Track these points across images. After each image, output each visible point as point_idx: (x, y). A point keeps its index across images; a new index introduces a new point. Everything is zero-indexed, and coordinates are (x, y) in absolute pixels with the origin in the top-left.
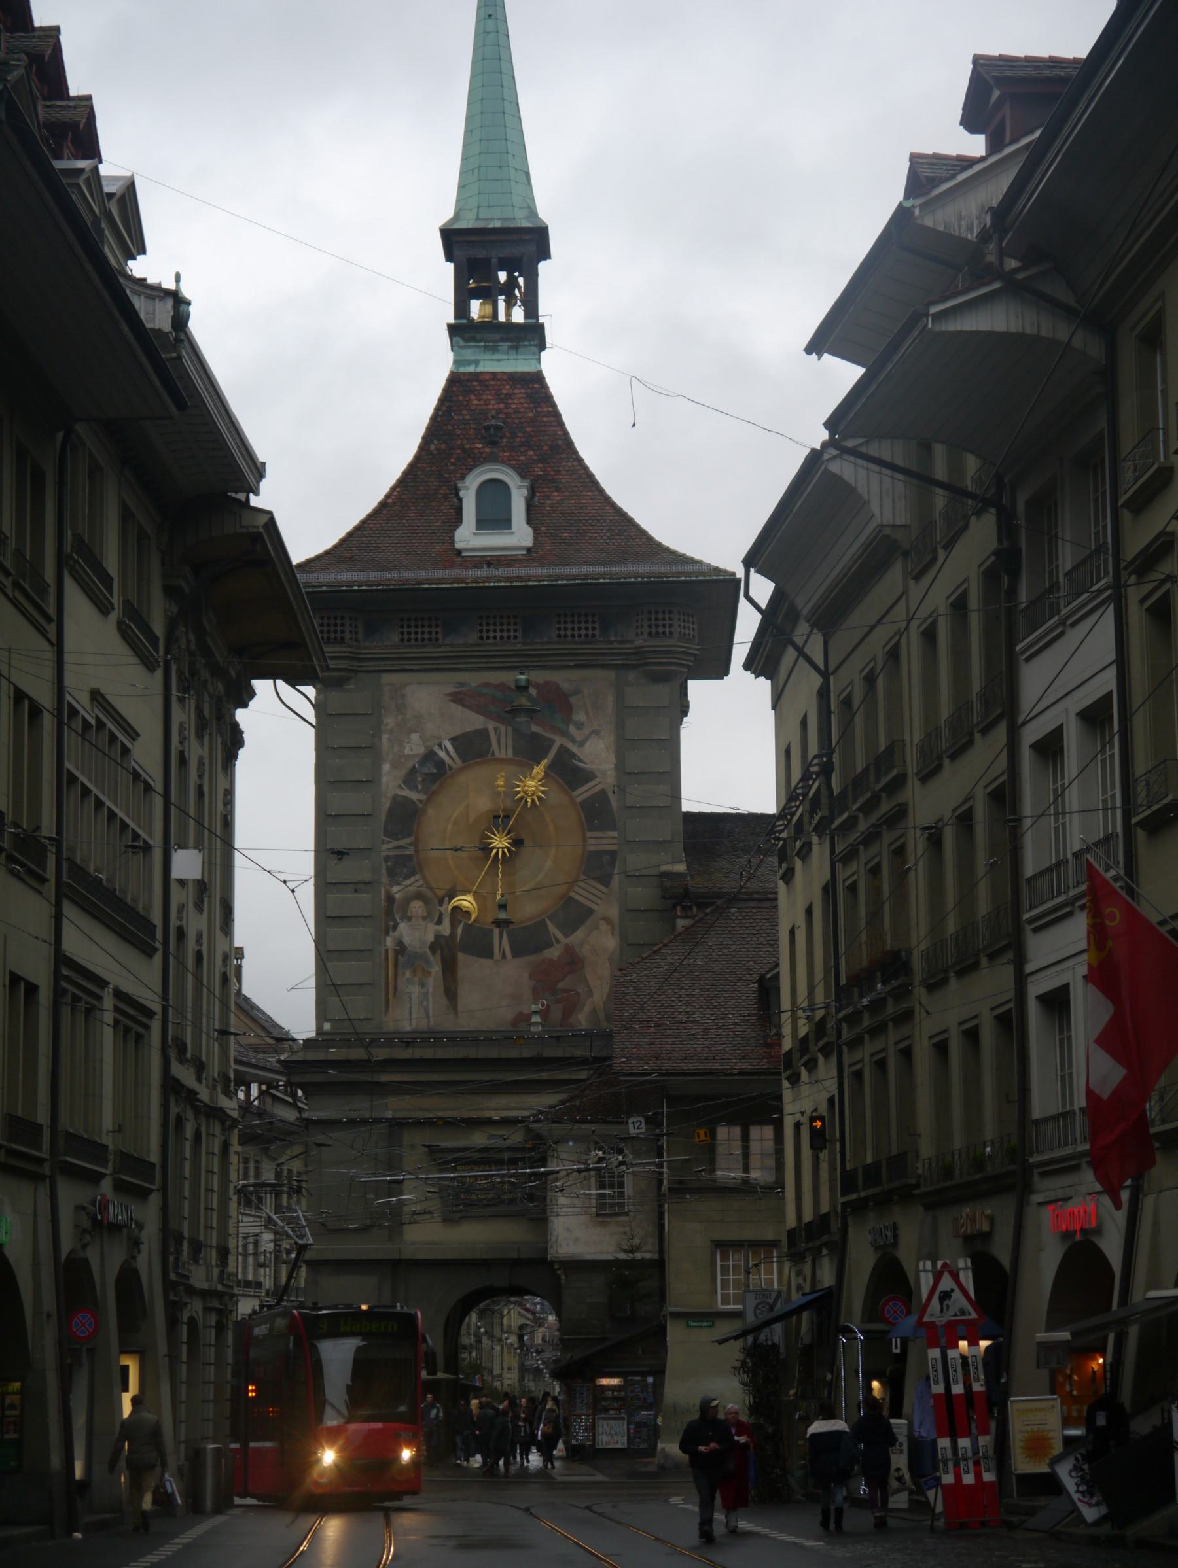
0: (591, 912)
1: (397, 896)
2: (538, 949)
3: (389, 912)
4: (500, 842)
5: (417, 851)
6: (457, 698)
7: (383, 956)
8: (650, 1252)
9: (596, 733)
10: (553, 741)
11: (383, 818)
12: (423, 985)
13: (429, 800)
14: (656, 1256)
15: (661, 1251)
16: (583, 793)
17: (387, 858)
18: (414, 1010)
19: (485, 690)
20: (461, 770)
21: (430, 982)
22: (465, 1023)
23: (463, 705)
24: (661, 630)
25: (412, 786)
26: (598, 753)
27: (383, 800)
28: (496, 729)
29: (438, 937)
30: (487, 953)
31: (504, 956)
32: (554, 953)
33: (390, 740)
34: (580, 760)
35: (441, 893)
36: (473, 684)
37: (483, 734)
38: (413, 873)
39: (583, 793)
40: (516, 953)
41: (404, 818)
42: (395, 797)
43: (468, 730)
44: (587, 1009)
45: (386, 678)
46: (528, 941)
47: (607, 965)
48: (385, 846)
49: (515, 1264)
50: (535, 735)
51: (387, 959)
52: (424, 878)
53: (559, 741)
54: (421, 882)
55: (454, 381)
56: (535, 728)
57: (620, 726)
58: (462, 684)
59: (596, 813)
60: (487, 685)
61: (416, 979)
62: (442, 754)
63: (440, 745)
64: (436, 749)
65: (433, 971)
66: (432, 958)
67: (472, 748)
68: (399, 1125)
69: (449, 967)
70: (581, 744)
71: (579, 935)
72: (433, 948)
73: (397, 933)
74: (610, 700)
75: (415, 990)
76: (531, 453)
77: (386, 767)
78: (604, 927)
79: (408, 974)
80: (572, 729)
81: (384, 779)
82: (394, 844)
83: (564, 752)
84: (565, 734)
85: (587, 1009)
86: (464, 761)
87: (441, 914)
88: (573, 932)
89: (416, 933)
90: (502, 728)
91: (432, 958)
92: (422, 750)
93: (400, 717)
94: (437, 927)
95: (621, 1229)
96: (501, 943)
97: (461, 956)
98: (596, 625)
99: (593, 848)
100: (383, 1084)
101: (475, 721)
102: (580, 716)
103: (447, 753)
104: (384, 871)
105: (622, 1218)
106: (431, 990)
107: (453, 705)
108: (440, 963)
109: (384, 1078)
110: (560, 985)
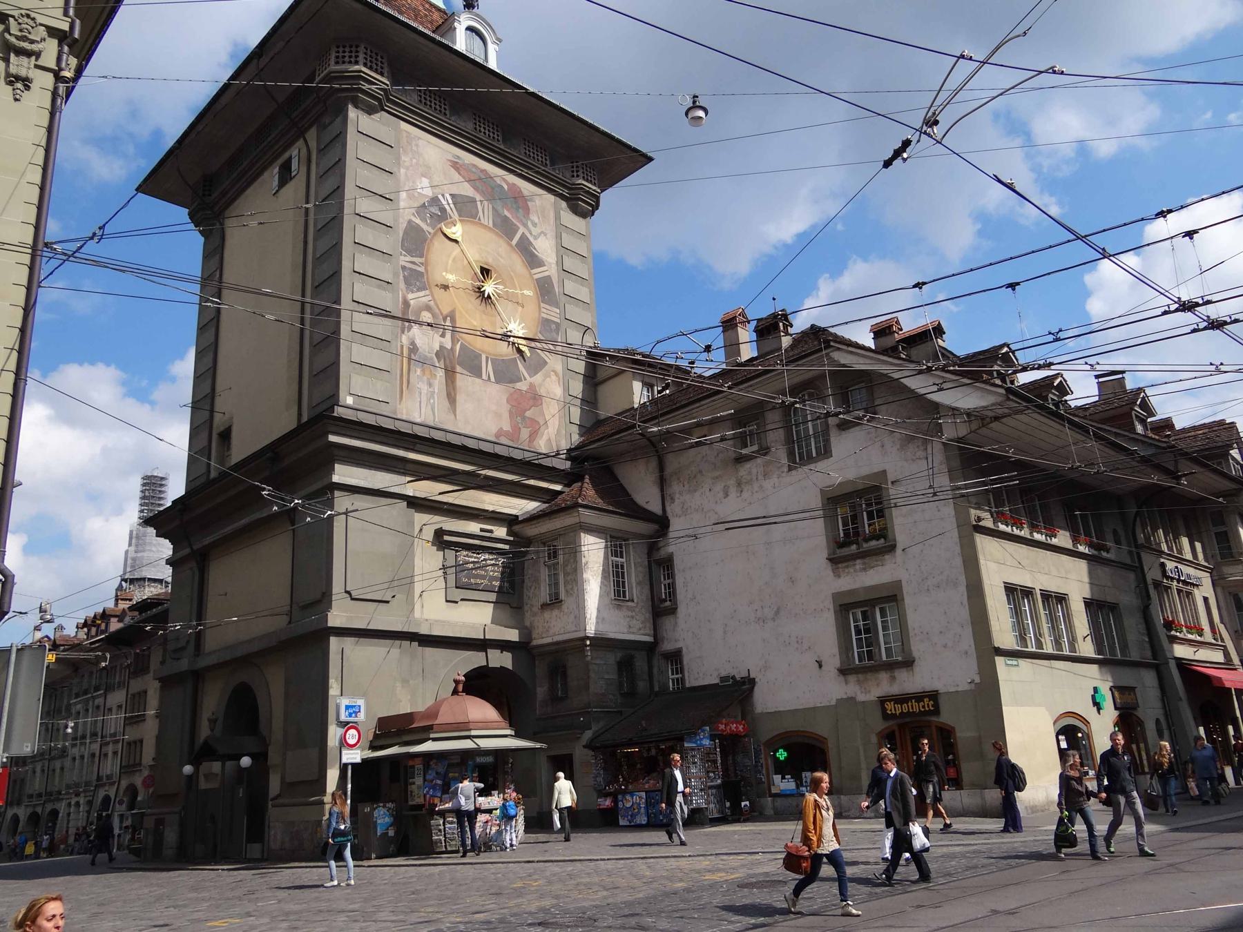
0: (546, 363)
1: (412, 302)
2: (512, 381)
6: (456, 166)
12: (430, 385)
15: (655, 636)
16: (538, 273)
17: (404, 268)
18: (423, 405)
25: (424, 220)
26: (545, 247)
30: (476, 371)
32: (522, 386)
35: (445, 312)
37: (473, 201)
38: (425, 289)
41: (415, 242)
44: (545, 437)
45: (403, 125)
48: (402, 258)
53: (522, 230)
54: (430, 298)
56: (506, 213)
57: (559, 237)
59: (545, 289)
62: (444, 202)
64: (440, 197)
68: (416, 504)
69: (450, 374)
70: (536, 238)
71: (538, 378)
72: (437, 354)
73: (411, 333)
74: (552, 214)
75: (424, 388)
77: (403, 195)
78: (554, 377)
79: (419, 371)
81: (402, 204)
82: (409, 258)
83: (523, 237)
84: (525, 226)
85: (545, 437)
88: (536, 373)
92: (430, 194)
96: (488, 369)
101: (467, 190)
102: (534, 218)
103: (447, 202)
105: (630, 604)
110: (528, 414)
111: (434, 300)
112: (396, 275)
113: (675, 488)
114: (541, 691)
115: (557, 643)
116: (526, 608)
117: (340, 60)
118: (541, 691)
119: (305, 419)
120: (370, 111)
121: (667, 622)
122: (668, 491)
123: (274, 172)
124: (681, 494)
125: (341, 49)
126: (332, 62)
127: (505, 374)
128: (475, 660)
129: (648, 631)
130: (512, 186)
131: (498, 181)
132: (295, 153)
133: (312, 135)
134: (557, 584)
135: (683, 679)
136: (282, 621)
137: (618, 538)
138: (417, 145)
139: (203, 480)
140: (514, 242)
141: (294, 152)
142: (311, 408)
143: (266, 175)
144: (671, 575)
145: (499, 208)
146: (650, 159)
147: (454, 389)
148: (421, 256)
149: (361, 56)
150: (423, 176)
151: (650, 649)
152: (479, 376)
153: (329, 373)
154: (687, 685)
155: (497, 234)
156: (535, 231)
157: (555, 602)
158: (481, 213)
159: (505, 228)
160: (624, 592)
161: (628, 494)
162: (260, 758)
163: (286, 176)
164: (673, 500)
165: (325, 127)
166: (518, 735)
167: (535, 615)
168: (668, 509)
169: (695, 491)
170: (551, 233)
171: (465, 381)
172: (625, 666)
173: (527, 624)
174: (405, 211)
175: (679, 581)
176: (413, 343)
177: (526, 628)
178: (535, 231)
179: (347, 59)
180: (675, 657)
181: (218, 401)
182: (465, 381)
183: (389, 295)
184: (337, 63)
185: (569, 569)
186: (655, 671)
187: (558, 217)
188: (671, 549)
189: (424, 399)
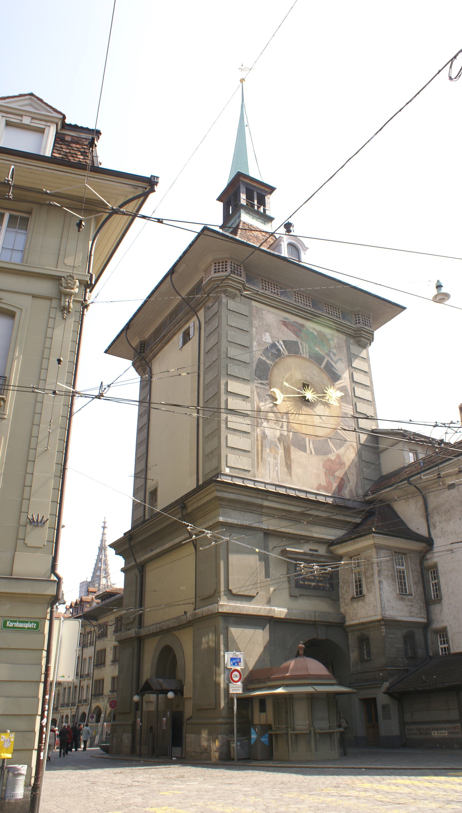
6: (285, 323)
7: (255, 439)
8: (424, 618)
9: (341, 360)
11: (254, 368)
12: (275, 458)
13: (274, 365)
14: (424, 620)
18: (271, 472)
19: (296, 325)
20: (287, 356)
21: (279, 457)
23: (287, 328)
24: (367, 323)
25: (268, 357)
27: (254, 359)
28: (301, 344)
29: (281, 435)
30: (303, 448)
31: (311, 453)
32: (332, 457)
33: (256, 332)
37: (296, 343)
40: (316, 454)
43: (290, 340)
45: (254, 303)
47: (355, 468)
49: (329, 625)
51: (257, 440)
58: (286, 318)
61: (272, 454)
62: (280, 347)
63: (278, 342)
65: (280, 453)
66: (279, 445)
70: (336, 363)
71: (342, 451)
72: (280, 439)
75: (271, 460)
77: (255, 344)
78: (352, 450)
79: (268, 450)
81: (254, 349)
83: (328, 363)
84: (328, 355)
85: (348, 489)
89: (272, 431)
91: (279, 445)
92: (271, 342)
93: (261, 323)
95: (410, 603)
96: (310, 446)
97: (292, 448)
99: (345, 411)
100: (261, 506)
101: (292, 337)
103: (282, 347)
104: (255, 393)
105: (410, 597)
106: (279, 462)
107: (283, 327)
108: (283, 449)
109: (266, 503)
112: (252, 392)
113: (435, 518)
114: (354, 655)
115: (363, 624)
116: (341, 600)
117: (217, 271)
118: (354, 655)
119: (201, 482)
120: (233, 297)
121: (435, 609)
122: (431, 521)
123: (179, 337)
124: (440, 522)
125: (217, 265)
126: (212, 272)
127: (322, 449)
128: (311, 635)
129: (423, 615)
130: (320, 332)
132: (192, 324)
133: (201, 313)
134: (361, 586)
135: (448, 648)
136: (190, 609)
137: (399, 553)
138: (262, 314)
139: (142, 520)
140: (322, 366)
141: (191, 324)
142: (204, 475)
143: (175, 338)
144: (436, 577)
146: (404, 308)
147: (290, 460)
148: (267, 379)
149: (229, 267)
150: (266, 331)
151: (426, 626)
152: (305, 451)
153: (215, 454)
154: (452, 652)
155: (312, 362)
156: (335, 359)
157: (360, 595)
158: (301, 351)
160: (406, 589)
161: (406, 525)
162: (179, 692)
163: (186, 338)
164: (435, 527)
165: (209, 308)
166: (340, 684)
167: (347, 605)
168: (432, 533)
169: (449, 520)
170: (345, 359)
172: (409, 638)
173: (342, 610)
174: (257, 353)
175: (443, 581)
176: (264, 433)
177: (342, 614)
178: (335, 359)
179: (221, 270)
180: (443, 633)
181: (149, 472)
182: (295, 454)
183: (249, 404)
184: (215, 272)
185: (368, 574)
186: (430, 642)
187: (348, 349)
188: (435, 560)
189: (272, 467)
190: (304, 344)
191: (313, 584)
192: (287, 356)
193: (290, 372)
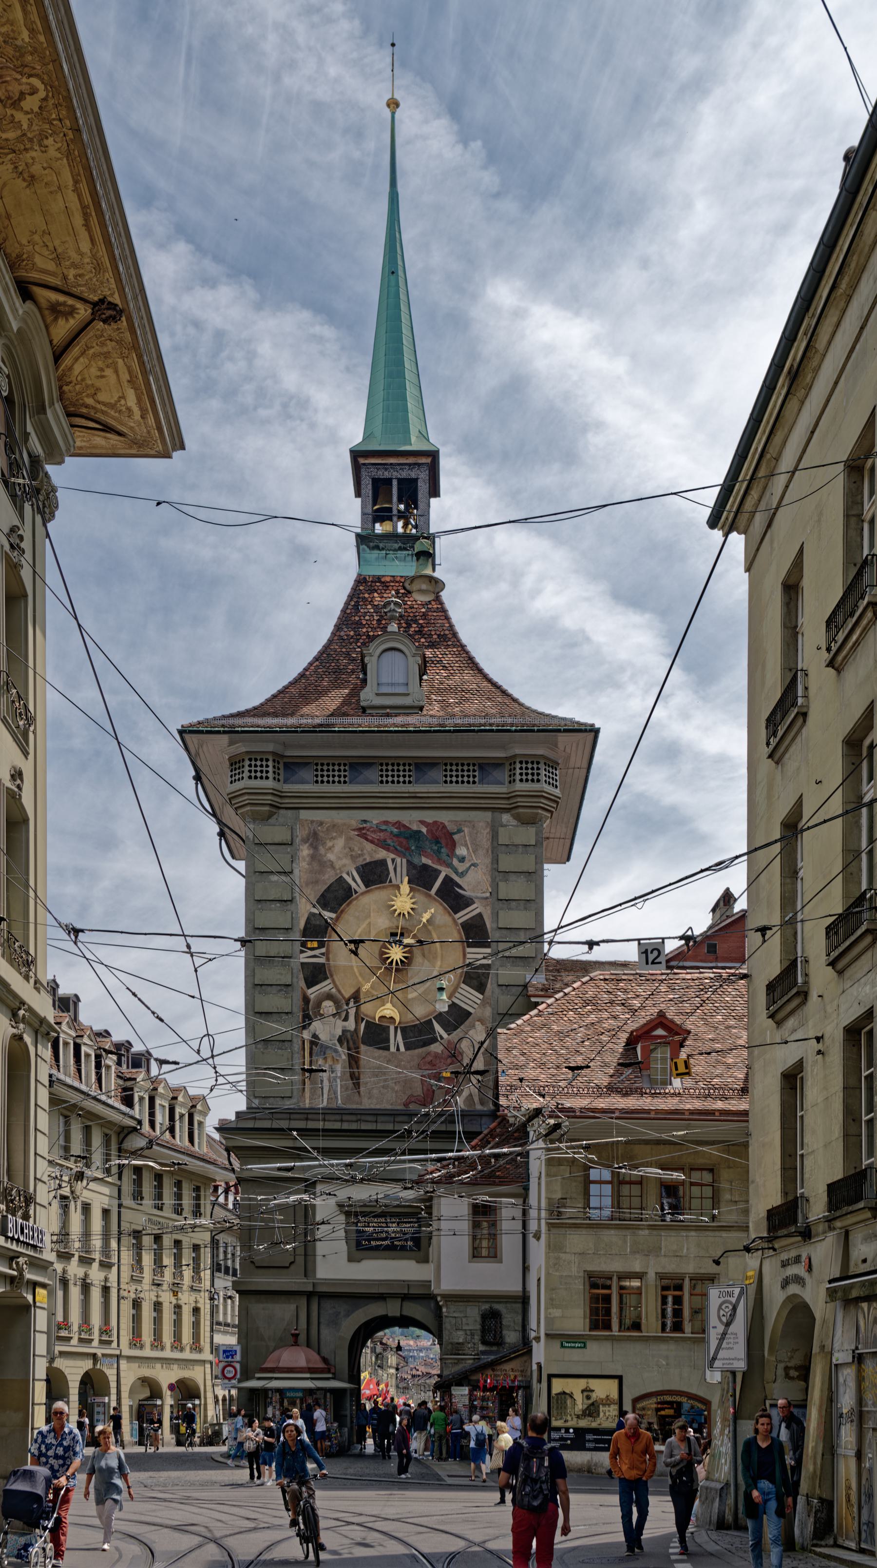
1: (312, 997)
3: (305, 1010)
4: (396, 953)
5: (328, 959)
10: (440, 872)
16: (464, 915)
19: (384, 827)
20: (363, 894)
22: (367, 1104)
28: (393, 860)
31: (398, 1049)
34: (460, 887)
35: (347, 996)
36: (375, 822)
37: (383, 863)
39: (464, 915)
42: (312, 915)
46: (418, 1034)
50: (425, 865)
52: (334, 982)
54: (331, 986)
55: (361, 581)
56: (425, 860)
57: (495, 860)
60: (386, 823)
62: (349, 880)
64: (345, 876)
66: (340, 1049)
67: (375, 875)
70: (462, 875)
72: (340, 1040)
73: (312, 1027)
76: (423, 640)
80: (455, 862)
83: (448, 880)
84: (449, 865)
86: (367, 886)
87: (347, 1013)
90: (398, 860)
94: (345, 1023)
97: (363, 1048)
98: (476, 773)
102: (461, 851)
111: (336, 986)
131: (415, 827)
145: (416, 861)
156: (461, 867)
159: (421, 878)
171: (369, 1056)
176: (315, 1036)
190: (398, 860)
191: (385, 1243)
192: (363, 894)
193: (367, 922)
